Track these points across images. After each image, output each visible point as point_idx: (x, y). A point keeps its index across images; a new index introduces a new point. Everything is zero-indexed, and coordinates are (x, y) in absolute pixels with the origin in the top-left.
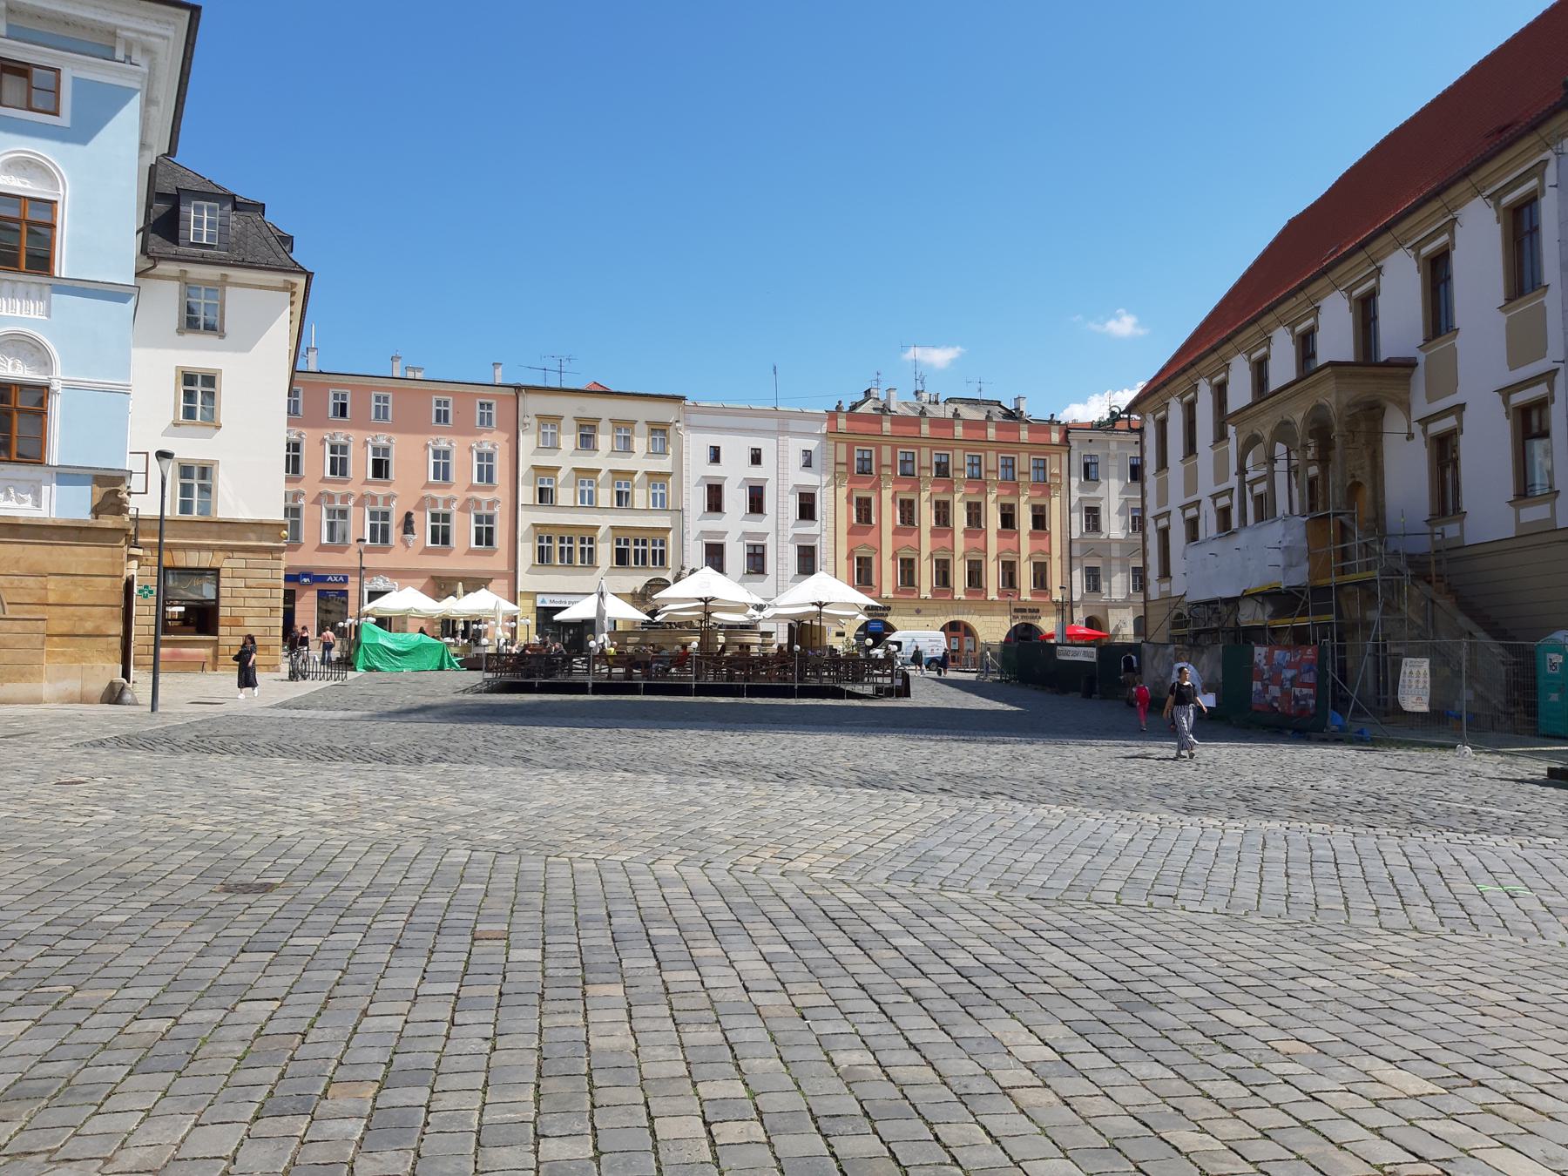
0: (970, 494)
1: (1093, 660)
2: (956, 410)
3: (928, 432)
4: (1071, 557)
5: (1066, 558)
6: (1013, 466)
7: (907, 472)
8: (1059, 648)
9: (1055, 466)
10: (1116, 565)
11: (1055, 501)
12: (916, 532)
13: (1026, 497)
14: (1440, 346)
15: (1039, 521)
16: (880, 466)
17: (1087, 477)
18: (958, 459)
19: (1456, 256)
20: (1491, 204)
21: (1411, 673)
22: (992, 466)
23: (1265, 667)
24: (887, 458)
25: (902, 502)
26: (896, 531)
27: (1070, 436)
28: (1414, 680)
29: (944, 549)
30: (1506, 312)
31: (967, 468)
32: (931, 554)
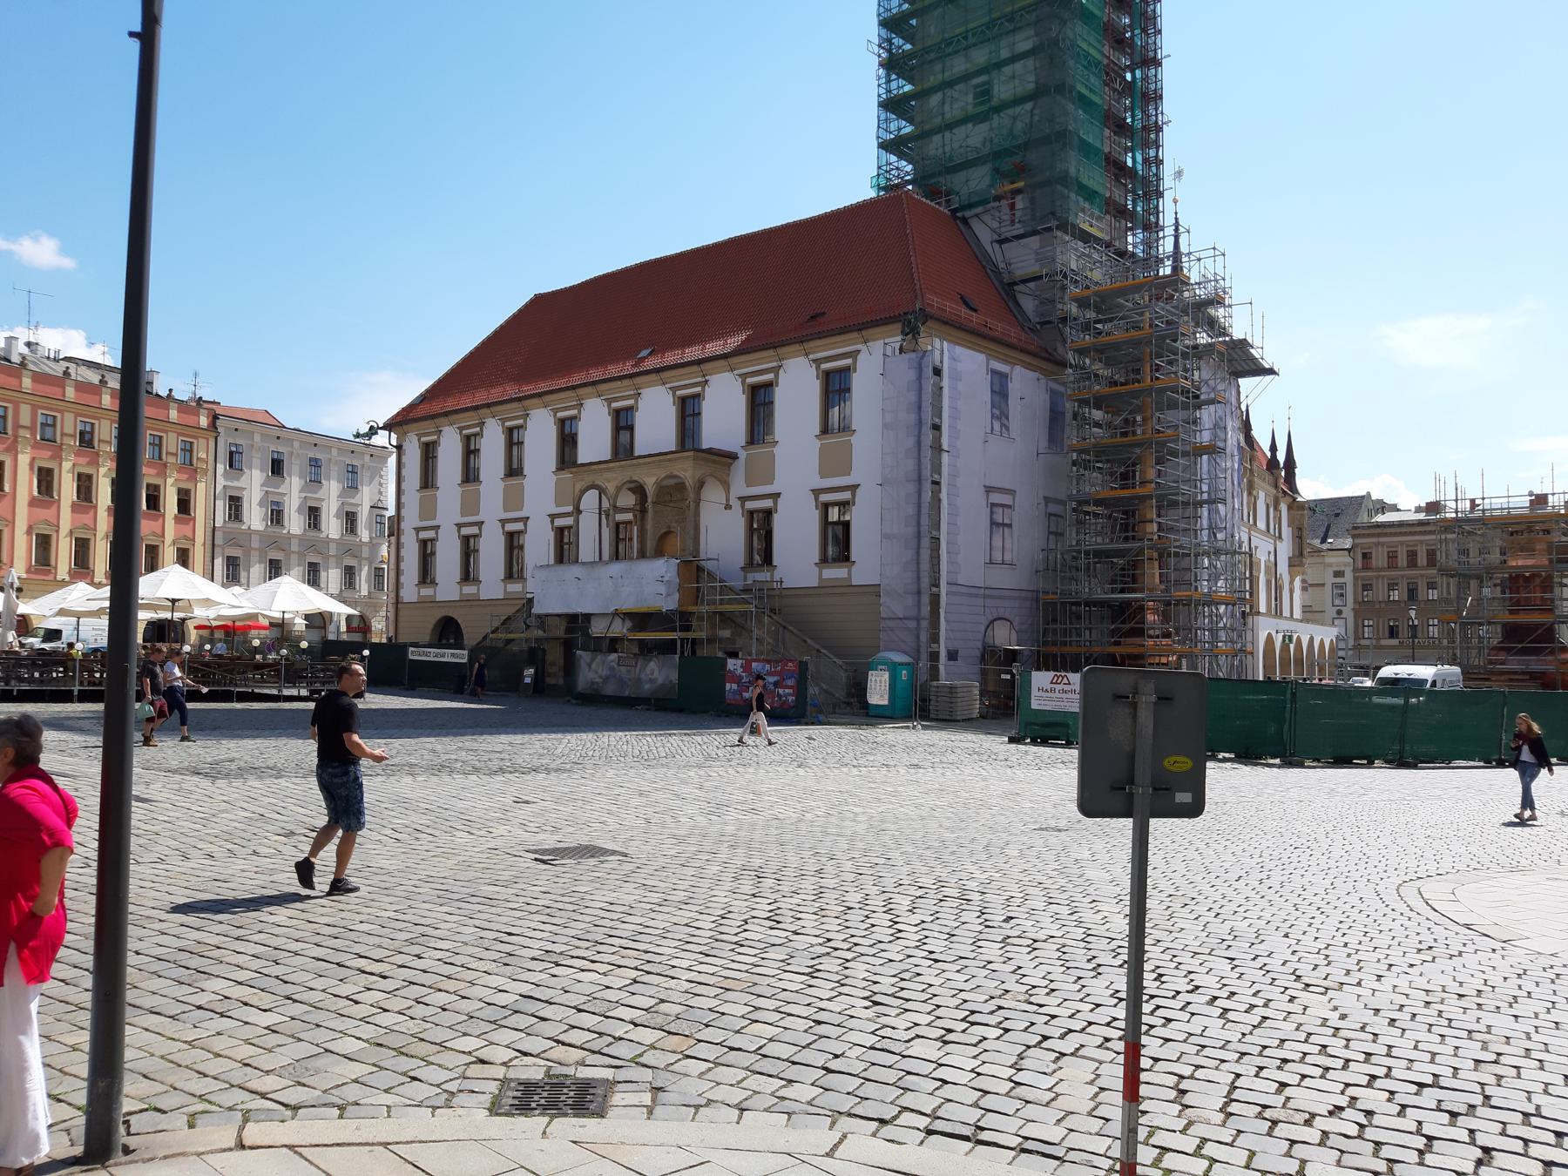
0: (182, 480)
1: (465, 661)
2: (68, 368)
4: (213, 545)
5: (209, 546)
6: (160, 446)
7: (48, 438)
8: (411, 649)
9: (202, 452)
10: (255, 555)
11: (201, 487)
13: (173, 479)
14: (758, 450)
15: (184, 505)
16: (17, 426)
17: (231, 466)
20: (814, 366)
24: (25, 419)
25: (40, 470)
26: (33, 503)
27: (218, 423)
29: (86, 527)
30: (820, 440)
32: (71, 531)
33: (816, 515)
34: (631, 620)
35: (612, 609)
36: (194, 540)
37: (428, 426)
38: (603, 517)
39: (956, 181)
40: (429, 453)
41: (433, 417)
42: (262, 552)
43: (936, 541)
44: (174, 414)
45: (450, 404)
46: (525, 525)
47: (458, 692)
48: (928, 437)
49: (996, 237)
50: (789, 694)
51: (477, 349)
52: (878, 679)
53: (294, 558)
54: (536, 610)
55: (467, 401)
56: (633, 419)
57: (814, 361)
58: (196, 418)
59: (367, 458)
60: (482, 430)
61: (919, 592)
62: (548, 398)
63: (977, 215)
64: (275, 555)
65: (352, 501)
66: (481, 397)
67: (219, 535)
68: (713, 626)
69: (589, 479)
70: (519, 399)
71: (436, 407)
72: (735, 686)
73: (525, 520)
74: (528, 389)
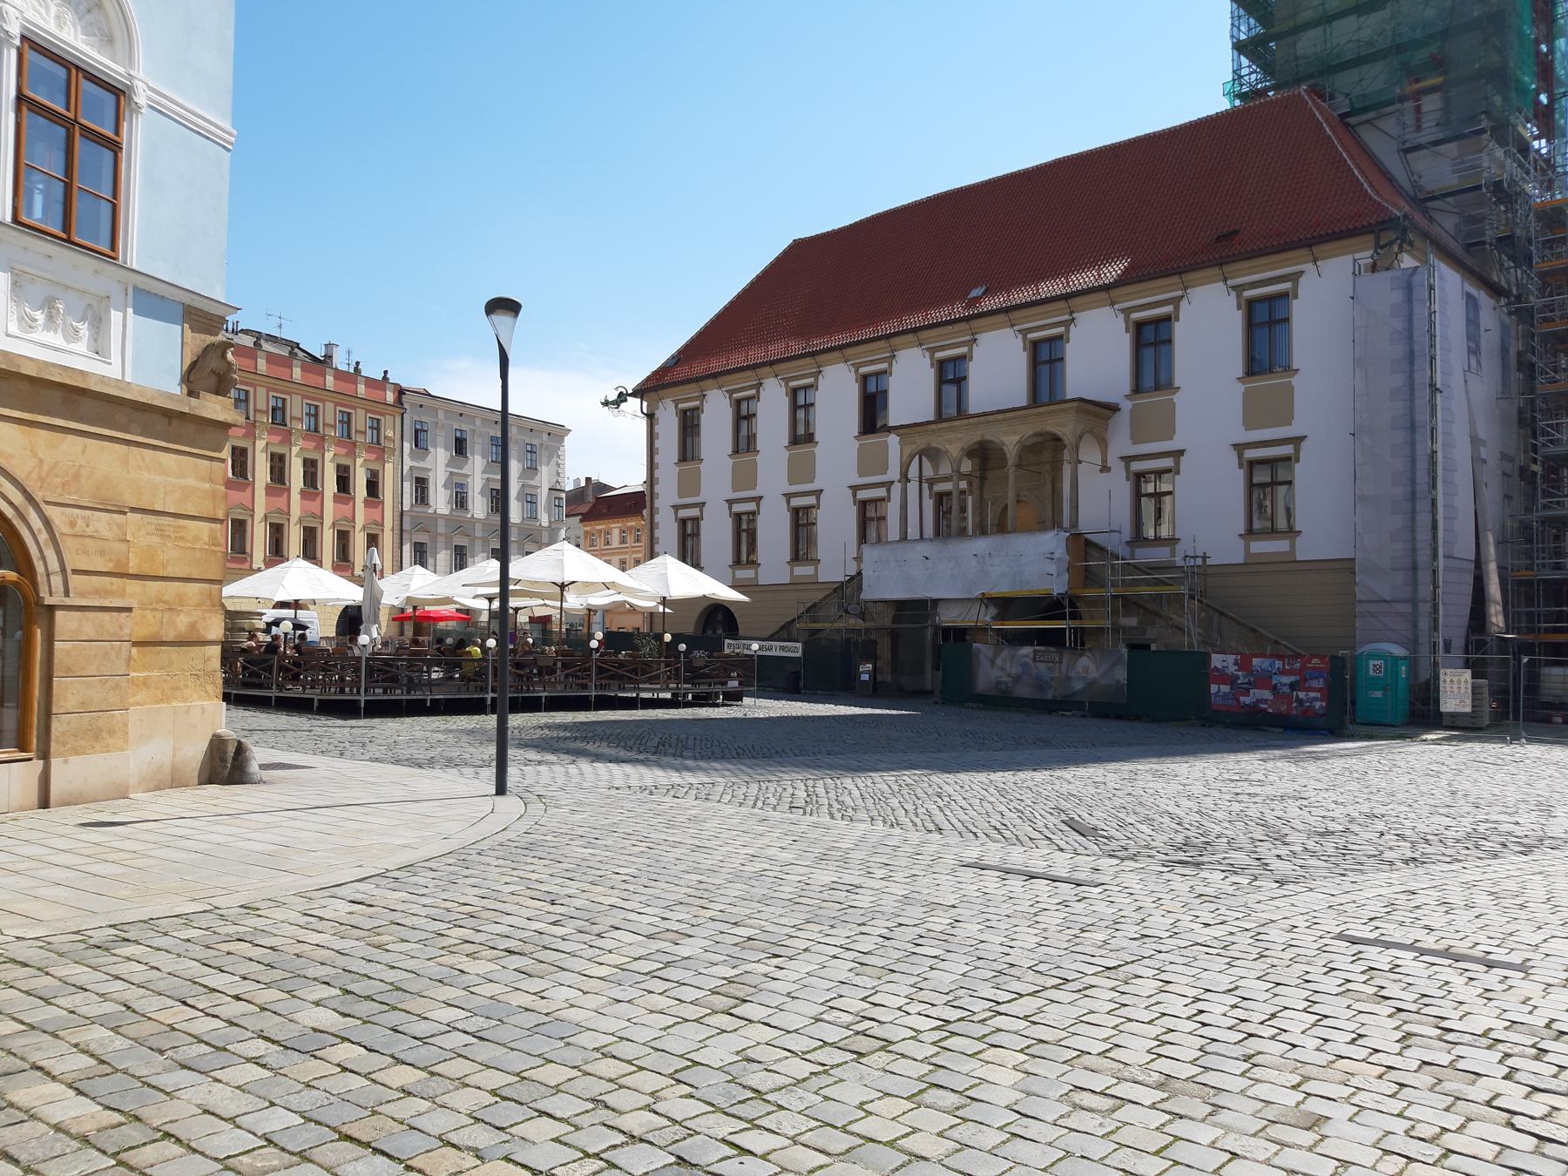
1: (799, 654)
3: (264, 369)
5: (397, 532)
11: (389, 467)
12: (250, 488)
15: (373, 487)
17: (416, 446)
18: (296, 406)
19: (1180, 331)
21: (1452, 681)
22: (330, 420)
23: (1240, 673)
28: (1455, 686)
29: (279, 511)
31: (305, 418)
33: (1240, 475)
34: (996, 606)
35: (977, 593)
36: (382, 525)
37: (692, 390)
38: (925, 486)
39: (1346, 81)
40: (689, 425)
41: (697, 380)
42: (448, 539)
43: (1434, 503)
44: (361, 389)
45: (716, 365)
46: (818, 499)
47: (792, 690)
48: (1422, 377)
49: (1401, 146)
50: (1316, 699)
51: (733, 304)
52: (1455, 679)
53: (478, 543)
54: (866, 595)
55: (737, 360)
56: (966, 370)
57: (1234, 288)
58: (383, 393)
59: (545, 436)
60: (758, 392)
61: (1415, 568)
62: (849, 351)
63: (1368, 121)
64: (460, 541)
65: (531, 482)
66: (756, 355)
67: (406, 520)
68: (1115, 612)
69: (921, 442)
70: (813, 354)
71: (698, 369)
72: (1225, 688)
73: (818, 493)
74: (818, 343)
